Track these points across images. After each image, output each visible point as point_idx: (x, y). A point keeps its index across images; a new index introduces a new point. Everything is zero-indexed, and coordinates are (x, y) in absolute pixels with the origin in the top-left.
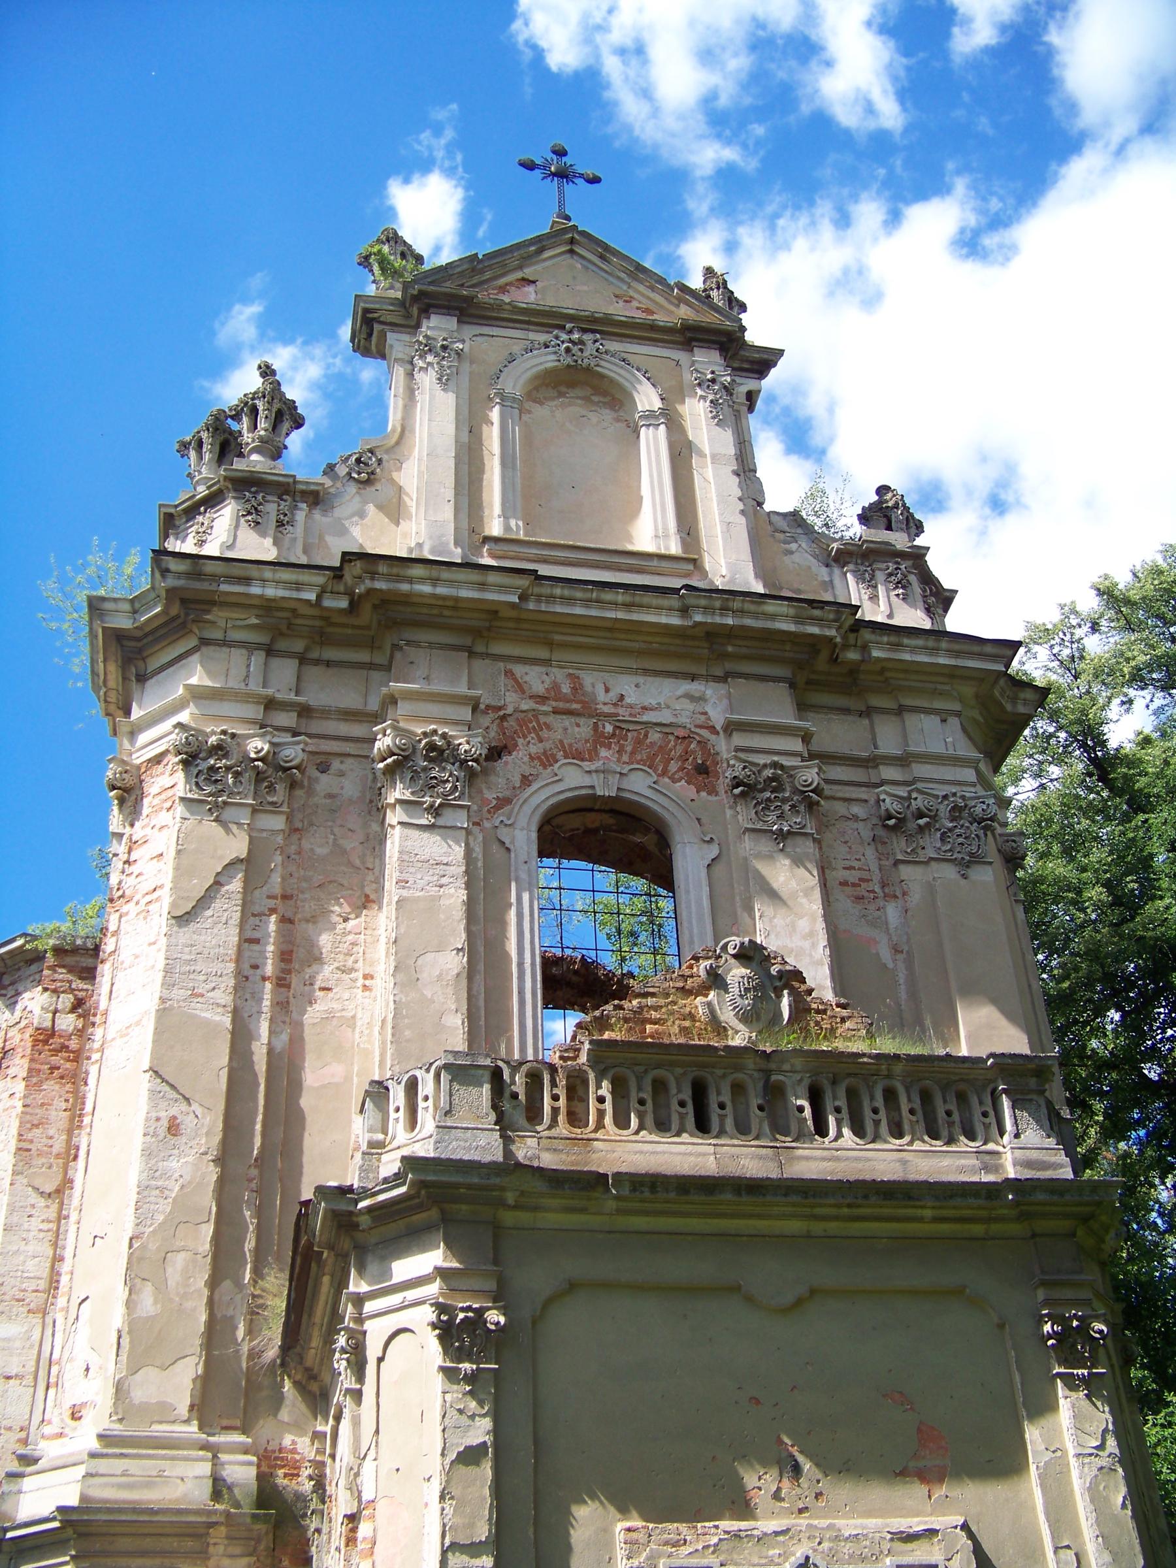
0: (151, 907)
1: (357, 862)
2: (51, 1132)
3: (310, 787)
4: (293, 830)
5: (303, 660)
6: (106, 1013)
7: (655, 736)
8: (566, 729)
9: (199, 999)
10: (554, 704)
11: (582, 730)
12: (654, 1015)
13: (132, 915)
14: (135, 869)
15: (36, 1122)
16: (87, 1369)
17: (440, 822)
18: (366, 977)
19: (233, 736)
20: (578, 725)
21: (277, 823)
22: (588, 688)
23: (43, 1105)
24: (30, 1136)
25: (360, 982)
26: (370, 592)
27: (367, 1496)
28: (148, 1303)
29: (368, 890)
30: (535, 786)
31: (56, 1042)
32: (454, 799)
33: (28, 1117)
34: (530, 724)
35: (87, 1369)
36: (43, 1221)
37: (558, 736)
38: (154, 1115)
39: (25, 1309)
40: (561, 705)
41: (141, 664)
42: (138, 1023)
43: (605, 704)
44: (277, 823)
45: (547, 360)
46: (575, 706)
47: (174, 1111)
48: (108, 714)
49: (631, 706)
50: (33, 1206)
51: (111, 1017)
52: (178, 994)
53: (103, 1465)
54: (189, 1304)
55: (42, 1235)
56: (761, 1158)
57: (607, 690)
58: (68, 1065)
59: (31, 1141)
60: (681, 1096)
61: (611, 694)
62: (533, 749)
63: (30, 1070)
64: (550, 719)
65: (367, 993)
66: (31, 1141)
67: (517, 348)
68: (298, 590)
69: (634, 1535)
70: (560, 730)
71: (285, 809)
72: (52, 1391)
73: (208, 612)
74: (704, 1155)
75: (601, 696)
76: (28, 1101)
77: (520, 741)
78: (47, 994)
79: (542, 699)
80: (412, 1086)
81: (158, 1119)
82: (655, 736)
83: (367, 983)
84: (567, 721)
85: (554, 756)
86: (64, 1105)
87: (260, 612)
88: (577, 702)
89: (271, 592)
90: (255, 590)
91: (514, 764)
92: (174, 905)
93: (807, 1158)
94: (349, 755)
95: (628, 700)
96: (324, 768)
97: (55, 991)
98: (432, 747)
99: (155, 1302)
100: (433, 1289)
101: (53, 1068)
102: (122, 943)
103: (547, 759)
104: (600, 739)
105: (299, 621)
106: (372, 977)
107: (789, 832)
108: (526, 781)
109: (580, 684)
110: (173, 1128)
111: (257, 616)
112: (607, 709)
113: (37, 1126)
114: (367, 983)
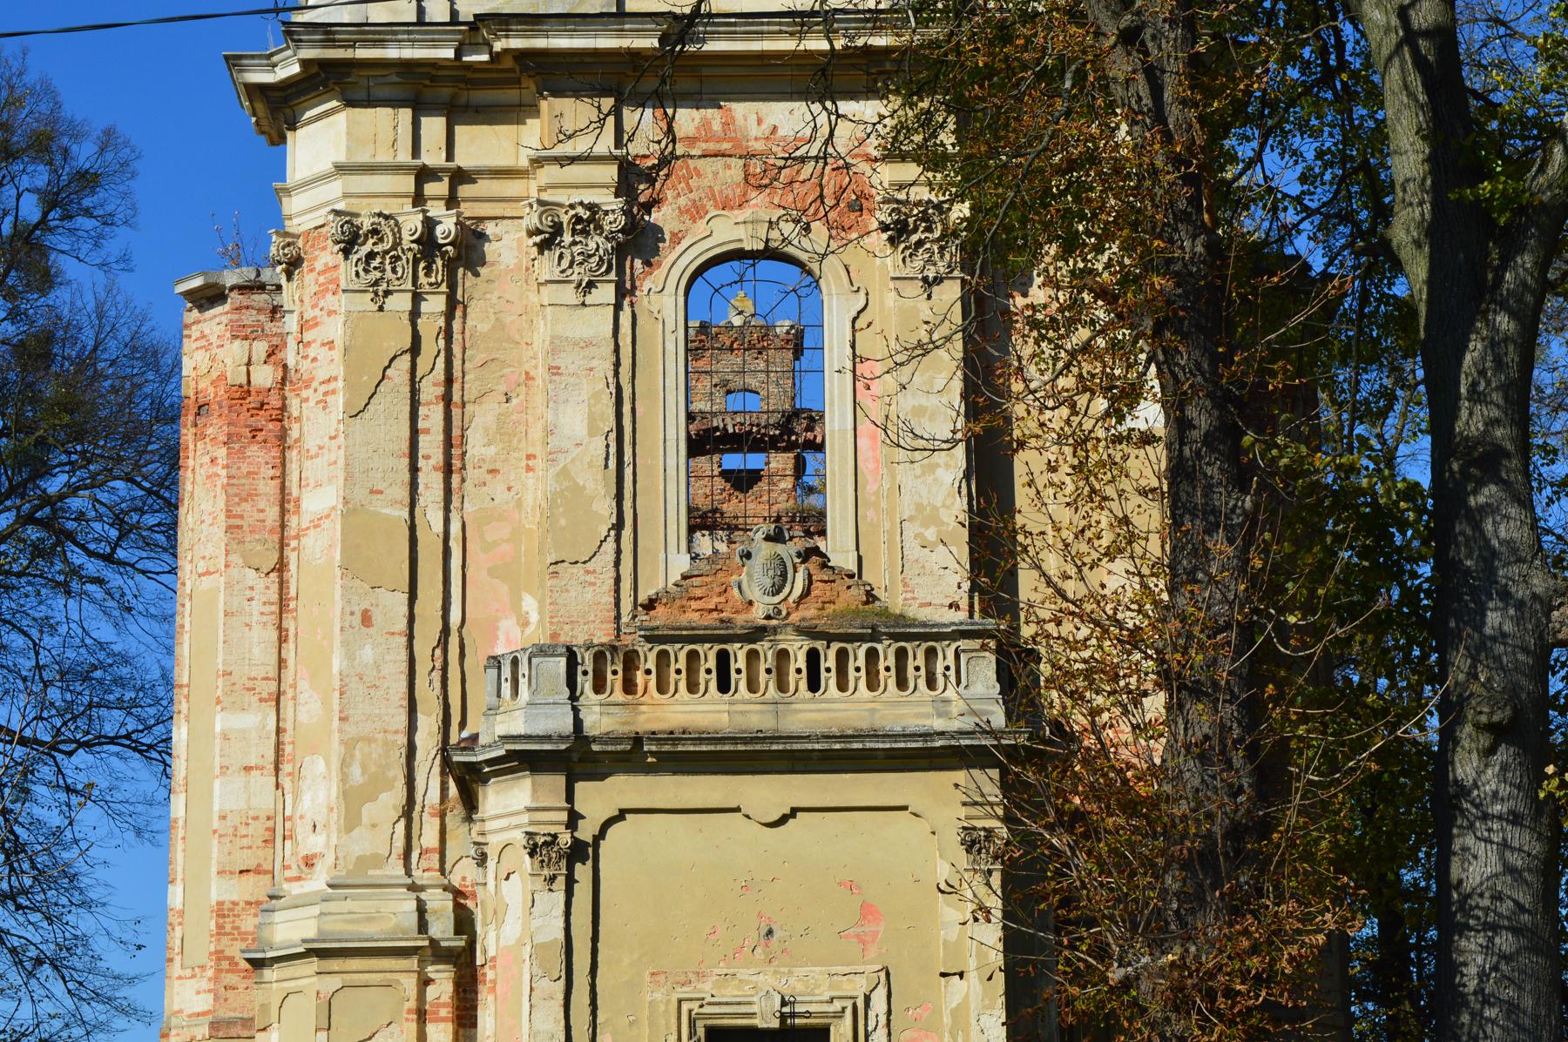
0: (328, 399)
1: (517, 338)
2: (262, 505)
3: (467, 258)
6: (298, 500)
8: (716, 174)
9: (379, 496)
10: (704, 146)
12: (698, 592)
13: (312, 403)
14: (312, 352)
15: (244, 494)
16: (315, 826)
17: (589, 299)
18: (529, 457)
19: (387, 217)
20: (729, 167)
22: (740, 121)
23: (249, 473)
24: (237, 510)
25: (524, 463)
26: (506, 51)
27: (491, 953)
29: (527, 367)
30: (685, 244)
31: (253, 401)
32: (601, 275)
33: (232, 491)
35: (315, 826)
36: (265, 603)
37: (706, 182)
38: (348, 610)
39: (256, 698)
40: (712, 146)
41: (288, 111)
42: (328, 516)
43: (756, 139)
46: (725, 146)
47: (365, 605)
48: (262, 133)
49: (784, 138)
50: (252, 588)
51: (304, 505)
52: (360, 494)
53: (332, 906)
54: (391, 774)
55: (265, 618)
56: (762, 712)
57: (760, 122)
58: (271, 426)
59: (241, 517)
60: (707, 666)
61: (764, 126)
62: (682, 201)
63: (229, 435)
64: (701, 163)
65: (531, 474)
66: (241, 517)
68: (435, 47)
69: (657, 978)
70: (710, 176)
71: (444, 288)
72: (288, 843)
73: (348, 75)
74: (719, 712)
75: (754, 131)
76: (233, 471)
77: (670, 194)
78: (237, 343)
80: (515, 663)
81: (352, 614)
83: (531, 463)
84: (720, 161)
85: (704, 206)
86: (271, 472)
87: (402, 70)
88: (731, 140)
89: (408, 53)
90: (392, 53)
92: (347, 404)
93: (801, 711)
94: (503, 218)
95: (781, 133)
97: (246, 338)
98: (579, 219)
99: (363, 774)
100: (525, 818)
101: (256, 431)
102: (305, 429)
103: (695, 212)
105: (441, 73)
106: (534, 457)
107: (935, 278)
109: (733, 118)
110: (366, 619)
111: (398, 74)
112: (758, 146)
113: (246, 500)
114: (531, 463)
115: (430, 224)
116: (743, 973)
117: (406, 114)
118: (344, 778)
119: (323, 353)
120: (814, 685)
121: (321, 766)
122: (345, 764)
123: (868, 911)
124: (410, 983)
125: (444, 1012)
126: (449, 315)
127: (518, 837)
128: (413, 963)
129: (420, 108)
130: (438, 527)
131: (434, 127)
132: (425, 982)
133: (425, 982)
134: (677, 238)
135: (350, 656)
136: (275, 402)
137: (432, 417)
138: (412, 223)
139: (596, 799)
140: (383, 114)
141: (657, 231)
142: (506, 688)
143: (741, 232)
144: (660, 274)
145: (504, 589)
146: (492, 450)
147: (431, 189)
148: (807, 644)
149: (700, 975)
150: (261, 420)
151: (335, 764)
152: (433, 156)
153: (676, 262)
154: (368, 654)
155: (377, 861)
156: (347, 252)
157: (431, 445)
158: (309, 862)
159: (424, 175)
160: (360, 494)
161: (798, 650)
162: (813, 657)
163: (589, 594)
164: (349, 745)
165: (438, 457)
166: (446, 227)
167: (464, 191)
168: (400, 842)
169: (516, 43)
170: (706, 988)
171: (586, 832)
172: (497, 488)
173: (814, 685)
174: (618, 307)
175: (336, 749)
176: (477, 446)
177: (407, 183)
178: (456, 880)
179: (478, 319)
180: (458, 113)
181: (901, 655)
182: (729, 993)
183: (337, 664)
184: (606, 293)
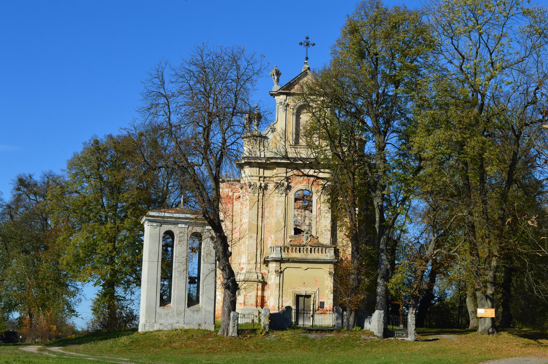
52: (251, 220)
103: (296, 184)
110: (251, 237)
115: (261, 184)
116: (301, 288)
117: (258, 169)
118: (248, 258)
120: (311, 252)
121: (244, 256)
122: (248, 256)
123: (317, 281)
124: (256, 285)
125: (260, 289)
126: (263, 196)
127: (274, 270)
128: (256, 283)
129: (260, 168)
130: (261, 225)
131: (262, 170)
132: (258, 285)
133: (258, 285)
134: (294, 187)
135: (249, 242)
136: (232, 198)
137: (260, 210)
138: (258, 184)
139: (284, 266)
140: (255, 169)
141: (291, 186)
142: (272, 251)
143: (302, 187)
144: (291, 192)
145: (269, 234)
146: (268, 215)
147: (261, 179)
148: (310, 247)
149: (296, 288)
150: (230, 200)
151: (247, 256)
152: (261, 175)
153: (293, 191)
154: (251, 242)
156: (250, 188)
157: (260, 214)
158: (242, 268)
159: (260, 177)
161: (309, 248)
162: (311, 249)
163: (281, 235)
164: (248, 254)
165: (261, 216)
166: (263, 185)
167: (265, 179)
168: (255, 267)
169: (273, 161)
170: (296, 290)
171: (282, 270)
172: (269, 220)
173: (311, 252)
174: (286, 197)
175: (247, 254)
176: (266, 214)
177: (258, 178)
178: (262, 272)
179: (267, 196)
180: (265, 168)
181: (322, 249)
182: (299, 290)
184: (284, 195)
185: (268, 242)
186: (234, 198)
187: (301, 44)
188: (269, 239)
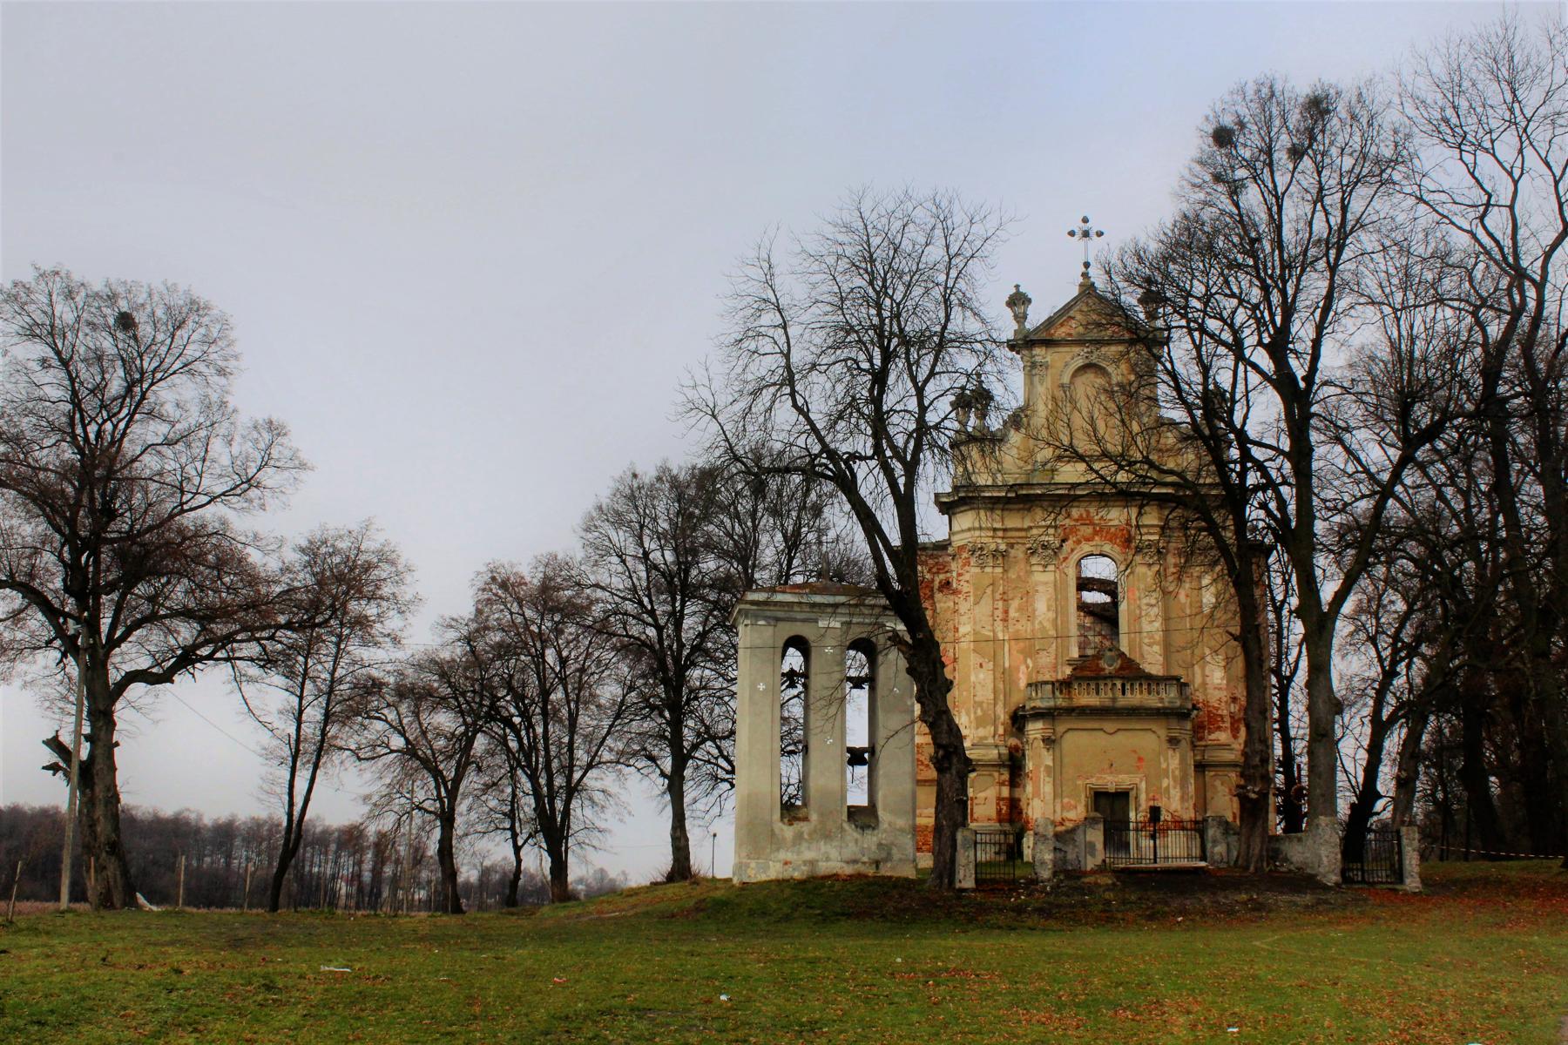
4: (1005, 571)
5: (1003, 510)
7: (1113, 529)
11: (1088, 530)
21: (999, 570)
28: (979, 712)
34: (1073, 530)
44: (999, 570)
45: (1080, 362)
67: (1068, 359)
79: (1077, 520)
82: (1113, 529)
91: (1067, 546)
96: (1012, 547)
103: (1078, 542)
104: (1096, 533)
108: (1072, 550)
110: (981, 666)
119: (966, 584)
120: (1124, 693)
123: (1140, 759)
127: (1038, 736)
154: (981, 676)
155: (986, 738)
160: (978, 628)
169: (1024, 492)
170: (1093, 780)
173: (1124, 693)
182: (1100, 782)
183: (973, 678)
185: (1021, 675)
186: (936, 584)
187: (1072, 234)
188: (1023, 668)
